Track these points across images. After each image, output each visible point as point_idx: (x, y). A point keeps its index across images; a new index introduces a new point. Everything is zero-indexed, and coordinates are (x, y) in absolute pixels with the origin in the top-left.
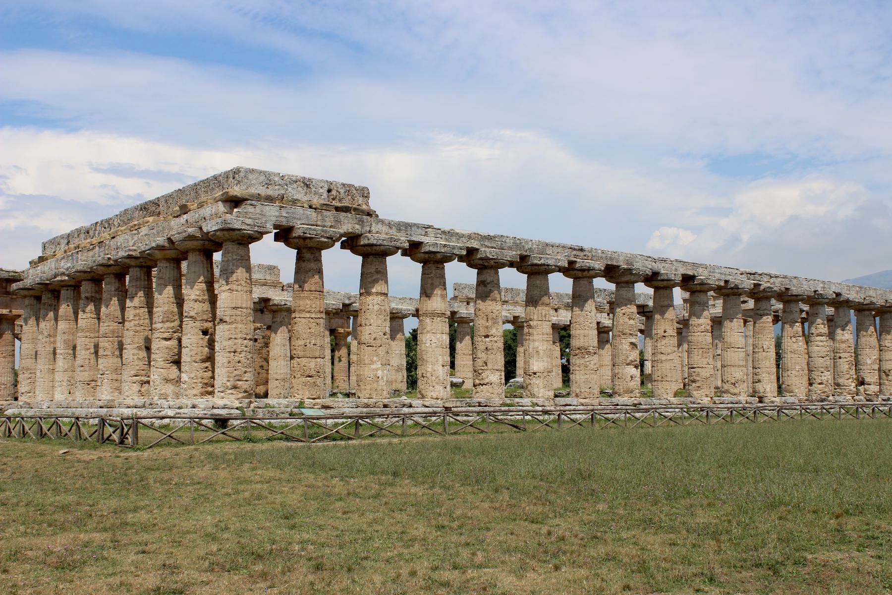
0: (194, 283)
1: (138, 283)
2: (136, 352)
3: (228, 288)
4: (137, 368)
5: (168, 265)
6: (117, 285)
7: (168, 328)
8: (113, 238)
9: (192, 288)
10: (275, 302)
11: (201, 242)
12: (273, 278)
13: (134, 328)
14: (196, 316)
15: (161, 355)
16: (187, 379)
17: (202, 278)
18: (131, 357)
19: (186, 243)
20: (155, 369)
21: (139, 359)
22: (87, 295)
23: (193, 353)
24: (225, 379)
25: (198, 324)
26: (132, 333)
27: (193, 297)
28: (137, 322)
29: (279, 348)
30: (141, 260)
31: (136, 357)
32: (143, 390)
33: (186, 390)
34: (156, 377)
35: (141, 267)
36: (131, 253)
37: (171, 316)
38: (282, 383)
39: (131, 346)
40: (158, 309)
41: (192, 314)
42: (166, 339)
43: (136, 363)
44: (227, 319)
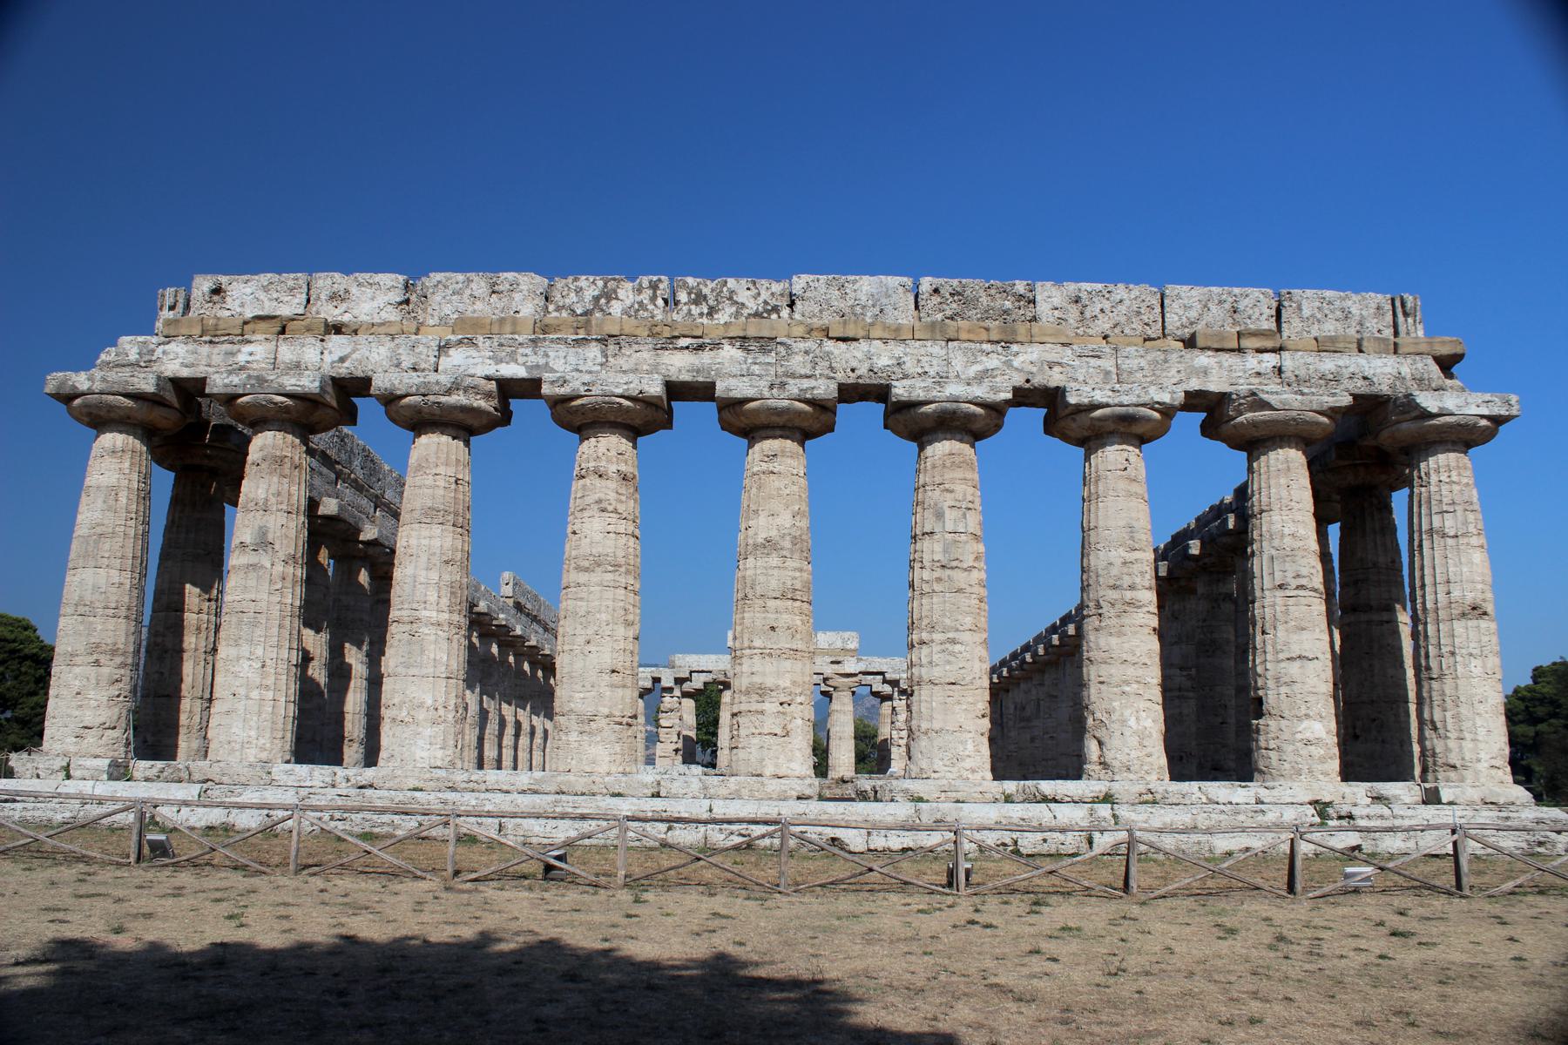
8: (844, 340)
20: (1142, 705)
22: (623, 468)
40: (1137, 555)
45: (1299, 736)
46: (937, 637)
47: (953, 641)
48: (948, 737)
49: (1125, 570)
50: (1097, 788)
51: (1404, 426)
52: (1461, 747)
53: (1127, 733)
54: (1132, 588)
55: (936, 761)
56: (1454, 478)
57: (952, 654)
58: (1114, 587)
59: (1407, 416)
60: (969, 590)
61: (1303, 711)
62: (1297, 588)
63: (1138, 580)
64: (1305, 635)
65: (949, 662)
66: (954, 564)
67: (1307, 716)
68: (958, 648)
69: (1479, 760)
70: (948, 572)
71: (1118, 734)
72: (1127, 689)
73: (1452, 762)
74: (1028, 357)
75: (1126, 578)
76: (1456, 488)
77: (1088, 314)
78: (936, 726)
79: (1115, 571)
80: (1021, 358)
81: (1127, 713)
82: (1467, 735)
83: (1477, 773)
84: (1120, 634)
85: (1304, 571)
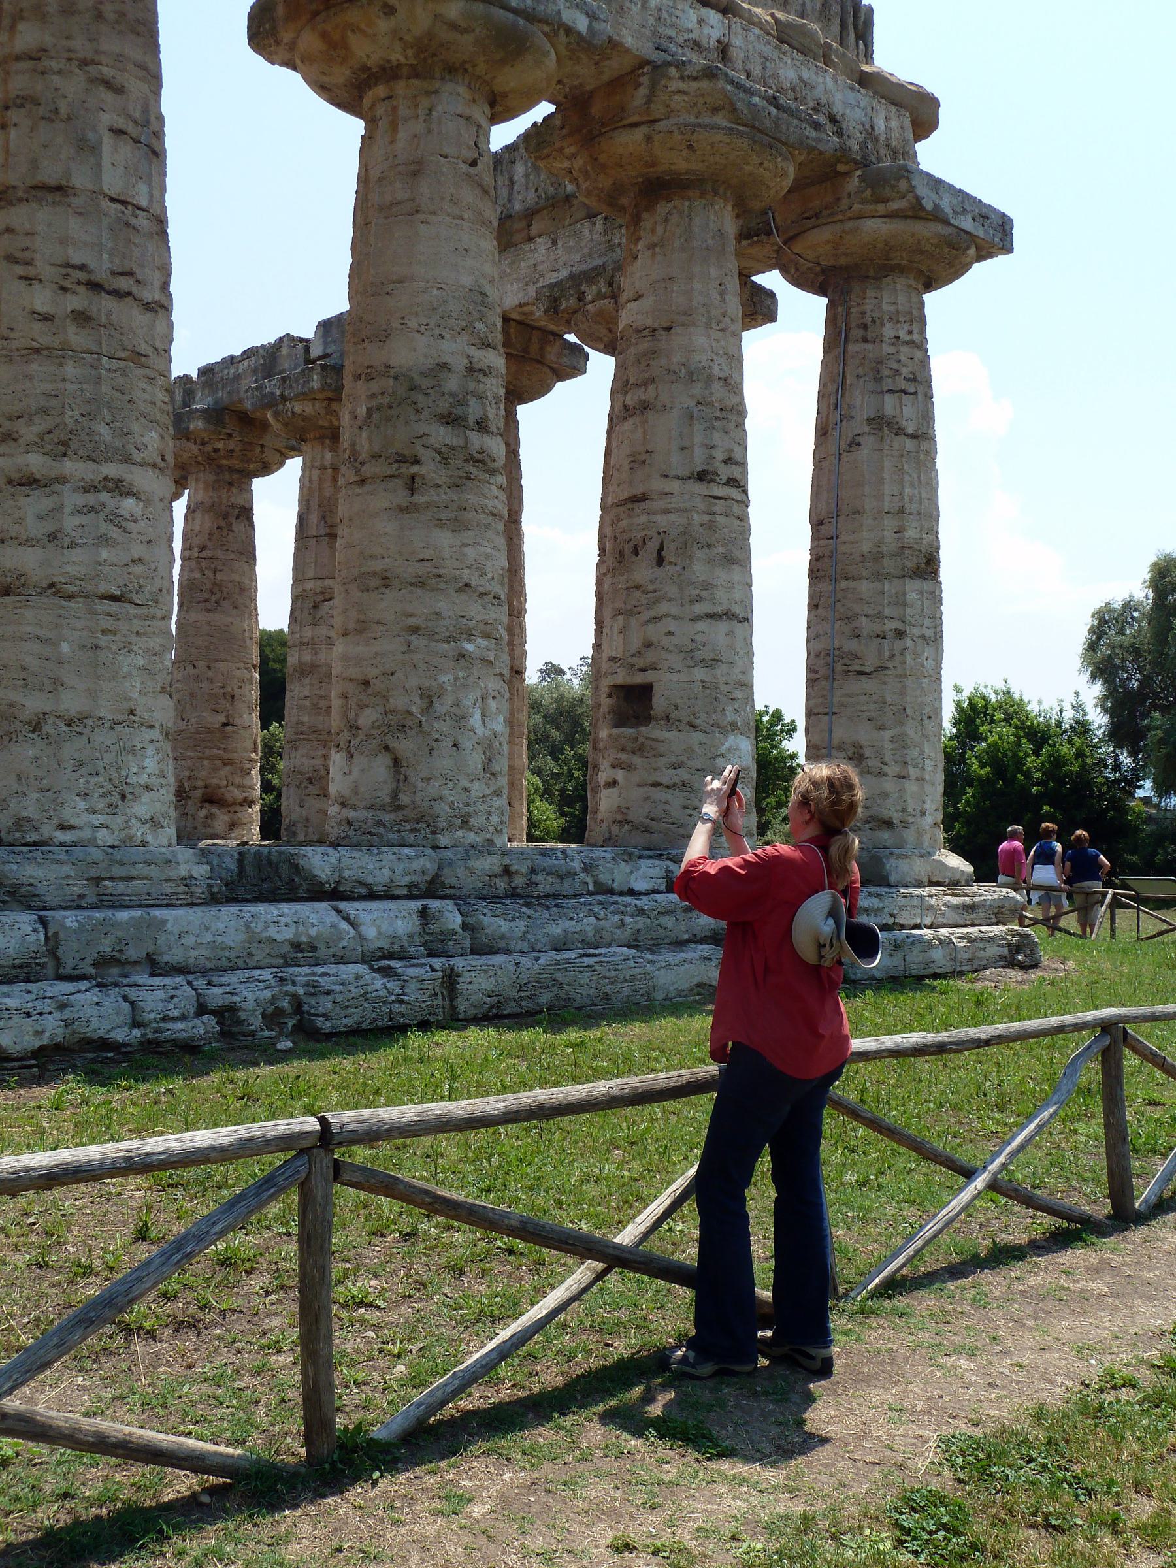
46: (71, 467)
47: (119, 488)
48: (102, 737)
49: (472, 386)
50: (417, 865)
51: (871, 224)
52: (902, 791)
53: (467, 744)
55: (70, 798)
57: (115, 518)
58: (451, 420)
59: (881, 208)
61: (730, 716)
65: (105, 540)
66: (123, 284)
68: (129, 504)
70: (107, 303)
71: (446, 744)
72: (469, 647)
73: (885, 814)
75: (472, 402)
78: (71, 703)
79: (452, 383)
81: (469, 699)
82: (913, 772)
84: (458, 526)
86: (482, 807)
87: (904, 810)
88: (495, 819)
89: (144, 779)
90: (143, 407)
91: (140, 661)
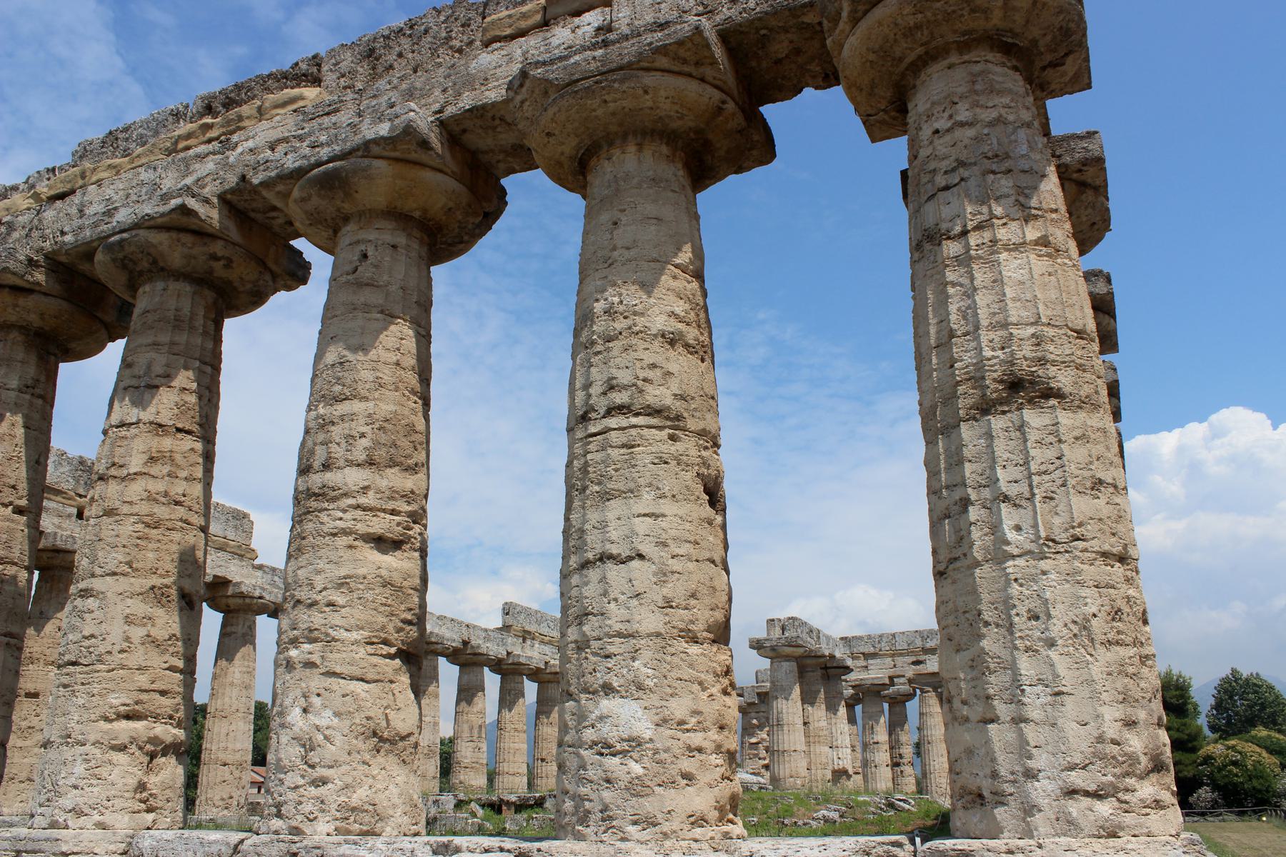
0: (660, 263)
1: (182, 338)
2: (138, 607)
3: (1032, 233)
4: (143, 680)
5: (401, 240)
6: (31, 371)
7: (394, 494)
8: (62, 196)
9: (647, 287)
10: (244, 589)
11: (717, 95)
12: (240, 539)
13: (144, 508)
14: (678, 406)
15: (358, 614)
16: (644, 728)
17: (685, 256)
18: (116, 630)
19: (649, 79)
20: (315, 682)
21: (151, 641)
23: (676, 589)
24: (1111, 714)
25: (688, 446)
26: (128, 528)
27: (659, 322)
28: (160, 486)
29: (235, 692)
30: (218, 248)
31: (137, 633)
32: (153, 780)
33: (636, 788)
34: (325, 719)
35: (201, 280)
36: (192, 203)
37: (404, 443)
38: (237, 774)
39: (123, 584)
41: (659, 395)
42: (382, 543)
43: (136, 658)
44: (1063, 379)
45: (589, 735)
49: (321, 437)
54: (326, 467)
56: (963, 114)
60: (125, 509)
61: (600, 678)
62: (609, 412)
63: (338, 452)
64: (615, 509)
67: (608, 689)
69: (1031, 775)
74: (250, 144)
76: (971, 132)
77: (380, 69)
80: (239, 150)
82: (1002, 709)
83: (1029, 809)
85: (624, 377)
86: (291, 796)
87: (995, 775)
88: (307, 807)
89: (72, 781)
90: (110, 540)
91: (81, 701)
